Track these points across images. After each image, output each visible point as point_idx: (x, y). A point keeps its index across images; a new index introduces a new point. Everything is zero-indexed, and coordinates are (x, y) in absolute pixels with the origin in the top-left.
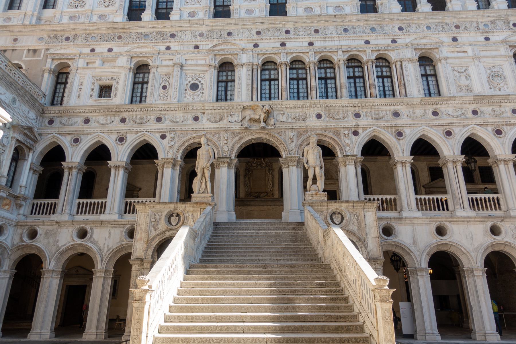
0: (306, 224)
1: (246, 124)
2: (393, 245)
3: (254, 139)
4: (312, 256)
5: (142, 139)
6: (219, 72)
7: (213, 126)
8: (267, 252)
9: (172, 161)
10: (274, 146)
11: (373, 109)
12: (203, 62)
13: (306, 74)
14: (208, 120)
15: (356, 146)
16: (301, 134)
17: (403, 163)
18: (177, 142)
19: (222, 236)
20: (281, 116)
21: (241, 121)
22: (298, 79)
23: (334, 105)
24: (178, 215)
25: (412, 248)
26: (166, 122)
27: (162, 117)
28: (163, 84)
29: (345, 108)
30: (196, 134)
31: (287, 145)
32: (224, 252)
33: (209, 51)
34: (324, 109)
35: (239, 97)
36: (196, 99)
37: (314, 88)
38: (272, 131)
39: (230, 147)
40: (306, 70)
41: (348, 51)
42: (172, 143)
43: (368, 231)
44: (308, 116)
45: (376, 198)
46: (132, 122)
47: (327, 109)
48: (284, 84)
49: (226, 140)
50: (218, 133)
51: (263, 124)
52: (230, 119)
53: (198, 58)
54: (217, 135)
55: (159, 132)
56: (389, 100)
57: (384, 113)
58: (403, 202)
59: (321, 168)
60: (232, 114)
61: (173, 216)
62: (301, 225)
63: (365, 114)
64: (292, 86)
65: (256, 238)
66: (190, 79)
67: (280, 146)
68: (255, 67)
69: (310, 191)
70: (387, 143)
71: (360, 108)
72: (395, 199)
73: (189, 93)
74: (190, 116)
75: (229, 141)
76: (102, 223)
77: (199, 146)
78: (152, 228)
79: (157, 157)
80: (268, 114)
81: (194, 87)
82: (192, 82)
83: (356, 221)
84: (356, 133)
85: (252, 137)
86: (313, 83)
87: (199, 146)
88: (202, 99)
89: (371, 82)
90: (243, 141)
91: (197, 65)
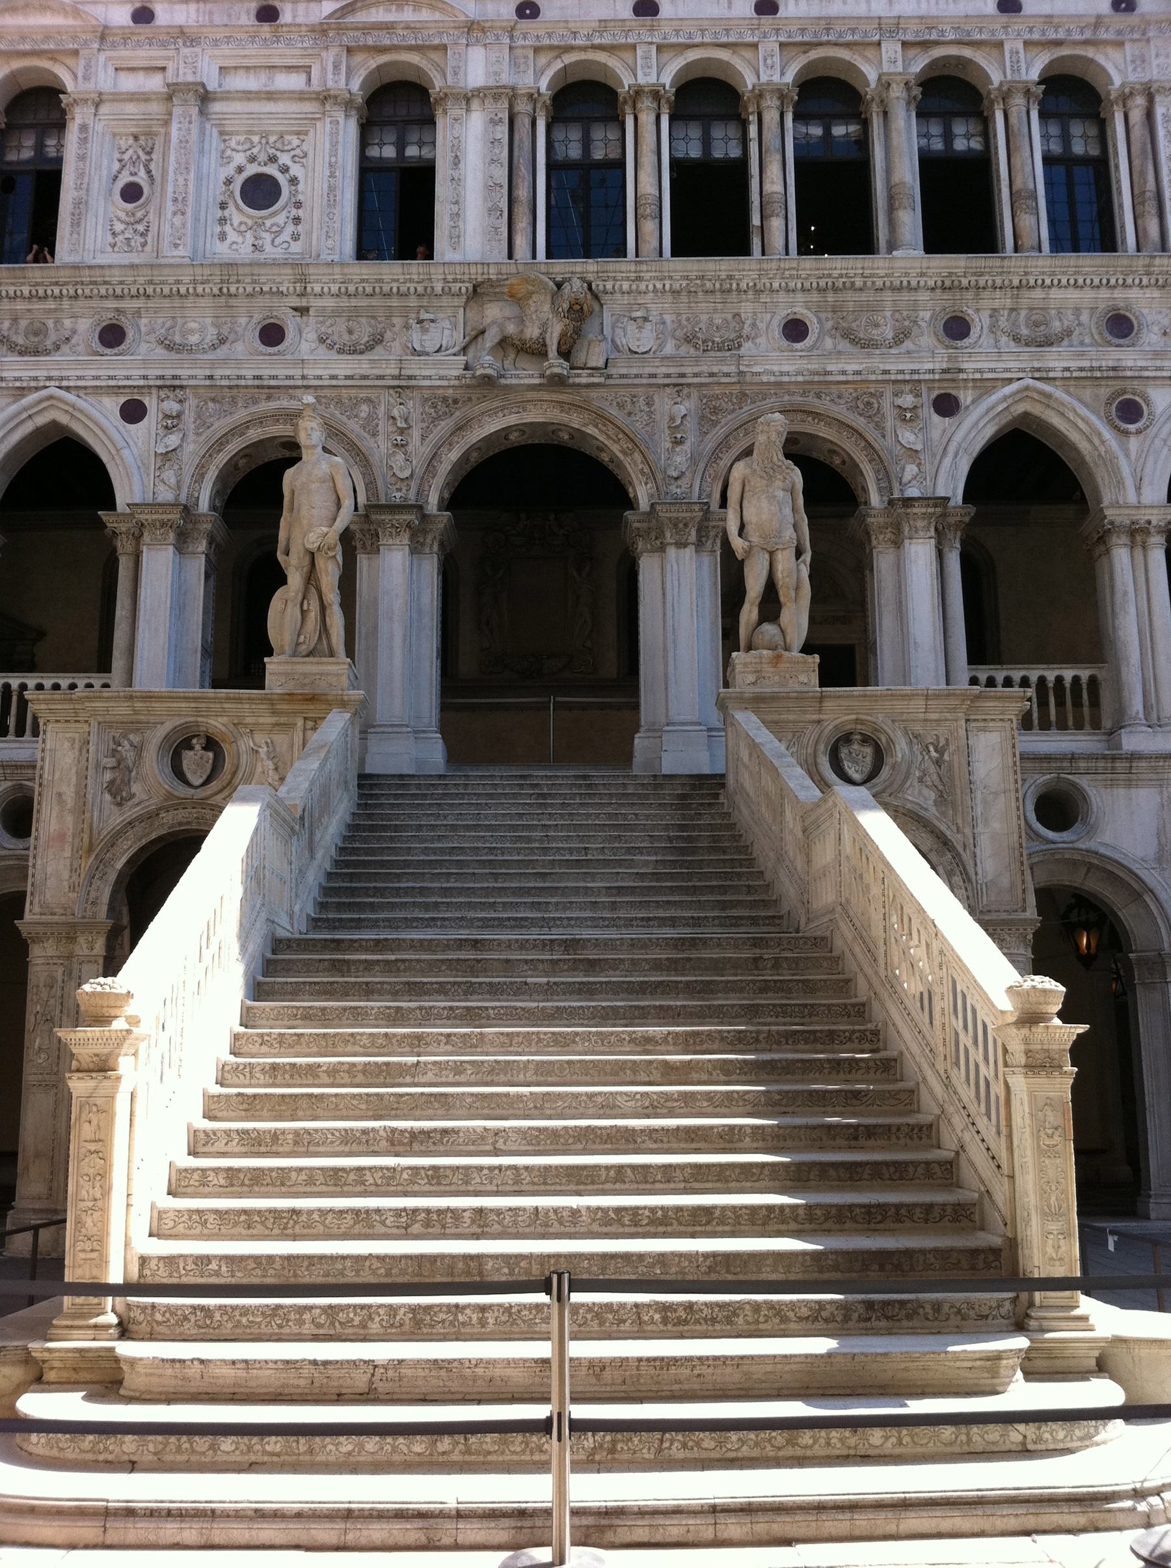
0: (731, 781)
1: (486, 362)
2: (1074, 863)
3: (521, 428)
4: (753, 905)
5: (41, 420)
6: (366, 129)
7: (344, 366)
8: (576, 891)
9: (175, 516)
10: (605, 457)
11: (1024, 302)
12: (295, 82)
13: (744, 141)
14: (322, 340)
16: (715, 410)
17: (1137, 533)
18: (191, 437)
19: (396, 828)
20: (631, 327)
21: (464, 350)
23: (859, 283)
24: (211, 744)
25: (1152, 877)
26: (144, 347)
27: (125, 322)
28: (125, 179)
29: (905, 296)
30: (273, 405)
31: (659, 463)
32: (408, 891)
33: (324, 32)
34: (815, 297)
35: (456, 239)
36: (268, 247)
37: (778, 208)
38: (594, 394)
39: (419, 463)
40: (744, 125)
41: (926, 45)
42: (173, 440)
43: (979, 810)
44: (747, 329)
45: (1017, 675)
47: (831, 297)
50: (369, 400)
51: (556, 365)
52: (416, 338)
53: (277, 61)
54: (365, 409)
55: (117, 390)
56: (1090, 263)
57: (1069, 319)
58: (1126, 694)
59: (799, 553)
60: (424, 316)
61: (191, 748)
62: (708, 787)
63: (986, 321)
65: (529, 840)
66: (240, 159)
67: (626, 461)
68: (523, 107)
69: (749, 648)
70: (1074, 448)
71: (969, 295)
72: (1093, 681)
73: (237, 219)
74: (243, 321)
75: (416, 434)
77: (291, 453)
78: (108, 797)
79: (109, 502)
80: (580, 314)
81: (260, 192)
82: (252, 170)
83: (932, 769)
84: (946, 406)
85: (512, 420)
87: (287, 454)
88: (296, 247)
89: (1018, 184)
90: (476, 434)
91: (271, 96)
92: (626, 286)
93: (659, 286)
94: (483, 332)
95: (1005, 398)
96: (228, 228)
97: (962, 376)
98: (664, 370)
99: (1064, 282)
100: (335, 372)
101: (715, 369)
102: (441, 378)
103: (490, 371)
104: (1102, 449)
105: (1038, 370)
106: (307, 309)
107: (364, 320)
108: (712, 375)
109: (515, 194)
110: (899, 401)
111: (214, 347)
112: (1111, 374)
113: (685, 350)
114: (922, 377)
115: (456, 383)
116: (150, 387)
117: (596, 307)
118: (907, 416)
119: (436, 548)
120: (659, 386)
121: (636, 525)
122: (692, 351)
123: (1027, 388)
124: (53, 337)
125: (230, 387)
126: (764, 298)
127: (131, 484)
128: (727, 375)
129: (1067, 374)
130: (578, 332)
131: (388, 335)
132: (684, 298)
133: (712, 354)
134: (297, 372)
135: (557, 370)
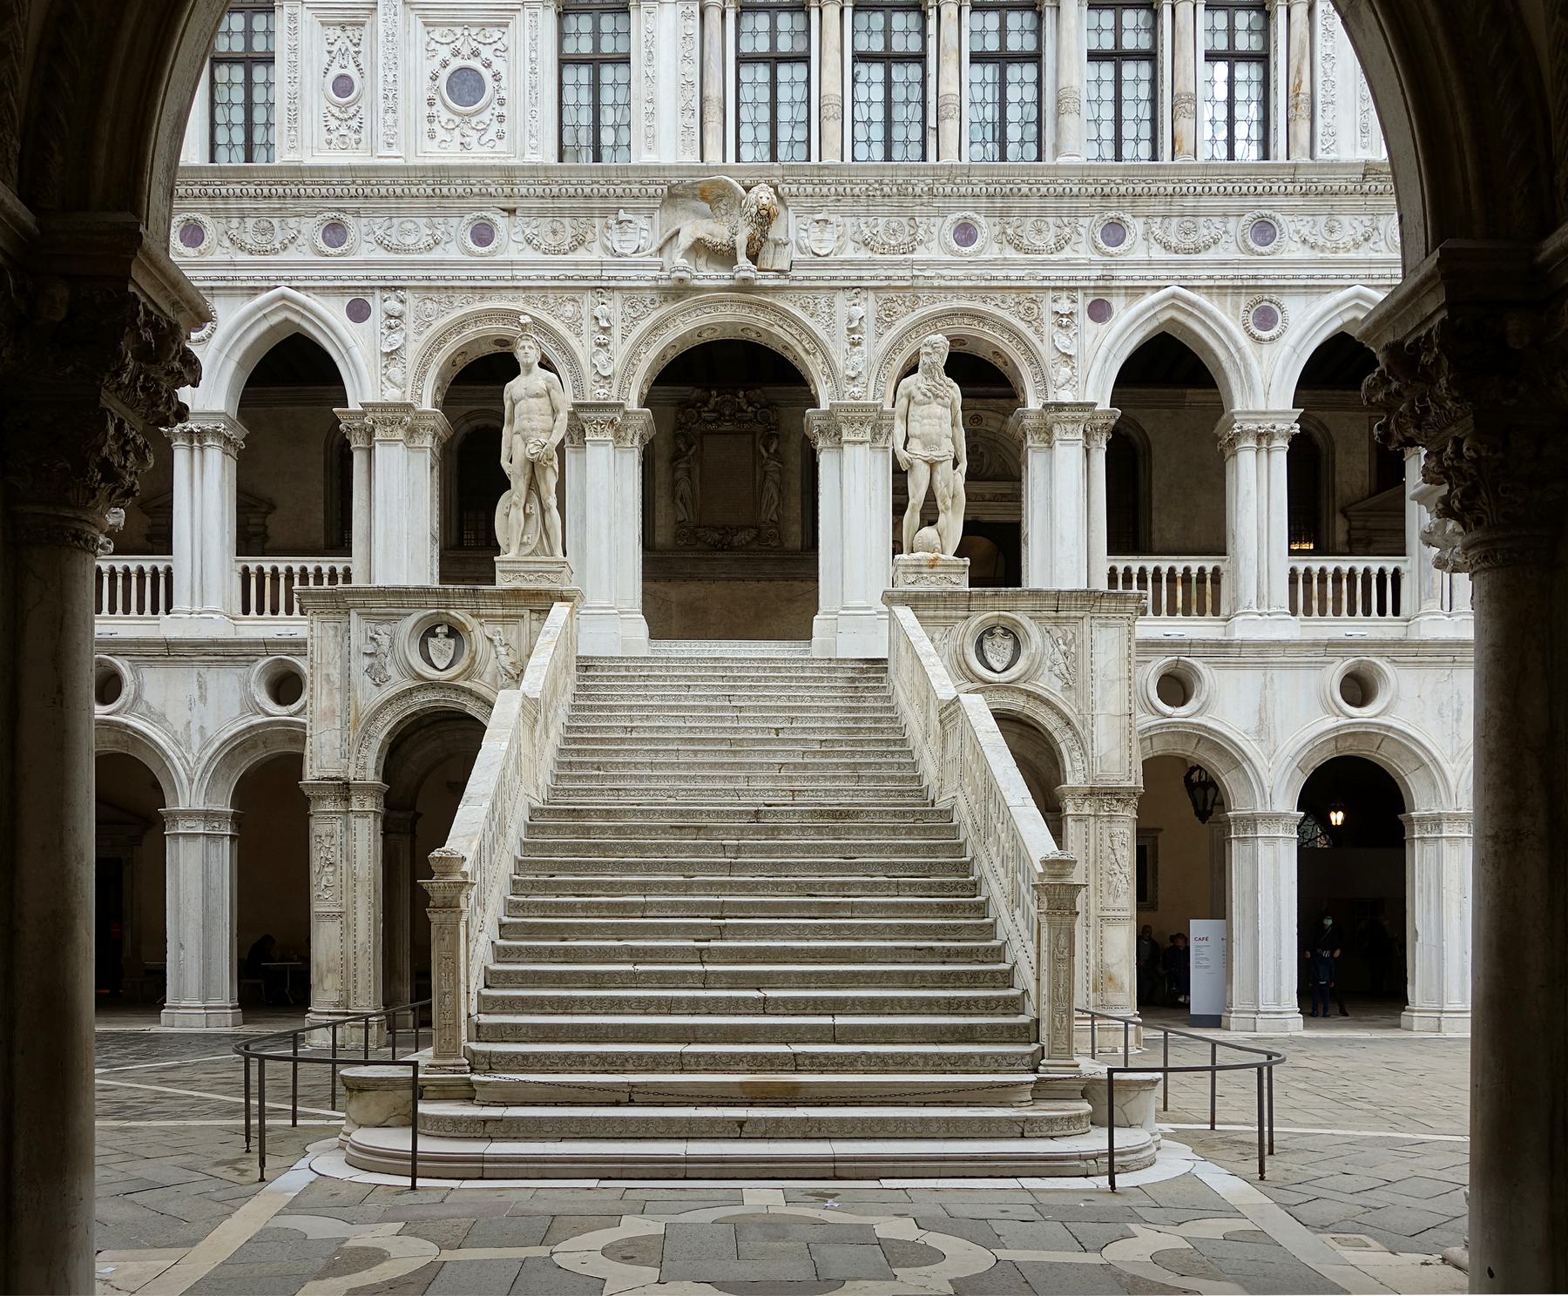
0: (891, 666)
14: (529, 242)
15: (1097, 366)
18: (412, 336)
20: (815, 229)
21: (660, 250)
22: (888, 59)
34: (984, 202)
35: (651, 139)
39: (619, 360)
46: (227, 243)
47: (999, 203)
48: (831, 86)
49: (605, 330)
60: (622, 215)
64: (862, 112)
71: (1126, 202)
75: (616, 332)
76: (170, 652)
79: (344, 402)
84: (1100, 311)
86: (950, 87)
90: (670, 335)
92: (809, 189)
93: (841, 189)
94: (678, 232)
95: (1153, 306)
96: (436, 126)
97: (1115, 283)
98: (845, 273)
99: (1214, 189)
100: (541, 273)
101: (890, 273)
102: (640, 279)
103: (683, 275)
104: (1237, 356)
105: (1185, 278)
106: (514, 211)
107: (566, 221)
108: (888, 278)
109: (706, 93)
110: (1057, 307)
111: (429, 248)
112: (1251, 283)
113: (864, 254)
114: (1079, 284)
115: (653, 283)
116: (372, 287)
117: (781, 209)
118: (1064, 321)
119: (636, 442)
120: (838, 288)
121: (816, 423)
122: (870, 254)
123: (1174, 296)
124: (279, 236)
125: (446, 288)
126: (938, 203)
127: (365, 383)
128: (901, 278)
129: (1211, 283)
130: (764, 234)
131: (589, 237)
132: (863, 199)
133: (888, 257)
134: (508, 274)
135: (743, 274)
